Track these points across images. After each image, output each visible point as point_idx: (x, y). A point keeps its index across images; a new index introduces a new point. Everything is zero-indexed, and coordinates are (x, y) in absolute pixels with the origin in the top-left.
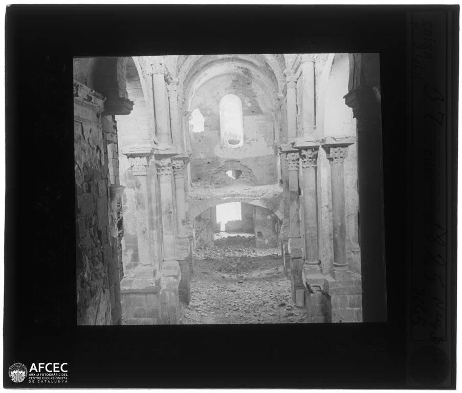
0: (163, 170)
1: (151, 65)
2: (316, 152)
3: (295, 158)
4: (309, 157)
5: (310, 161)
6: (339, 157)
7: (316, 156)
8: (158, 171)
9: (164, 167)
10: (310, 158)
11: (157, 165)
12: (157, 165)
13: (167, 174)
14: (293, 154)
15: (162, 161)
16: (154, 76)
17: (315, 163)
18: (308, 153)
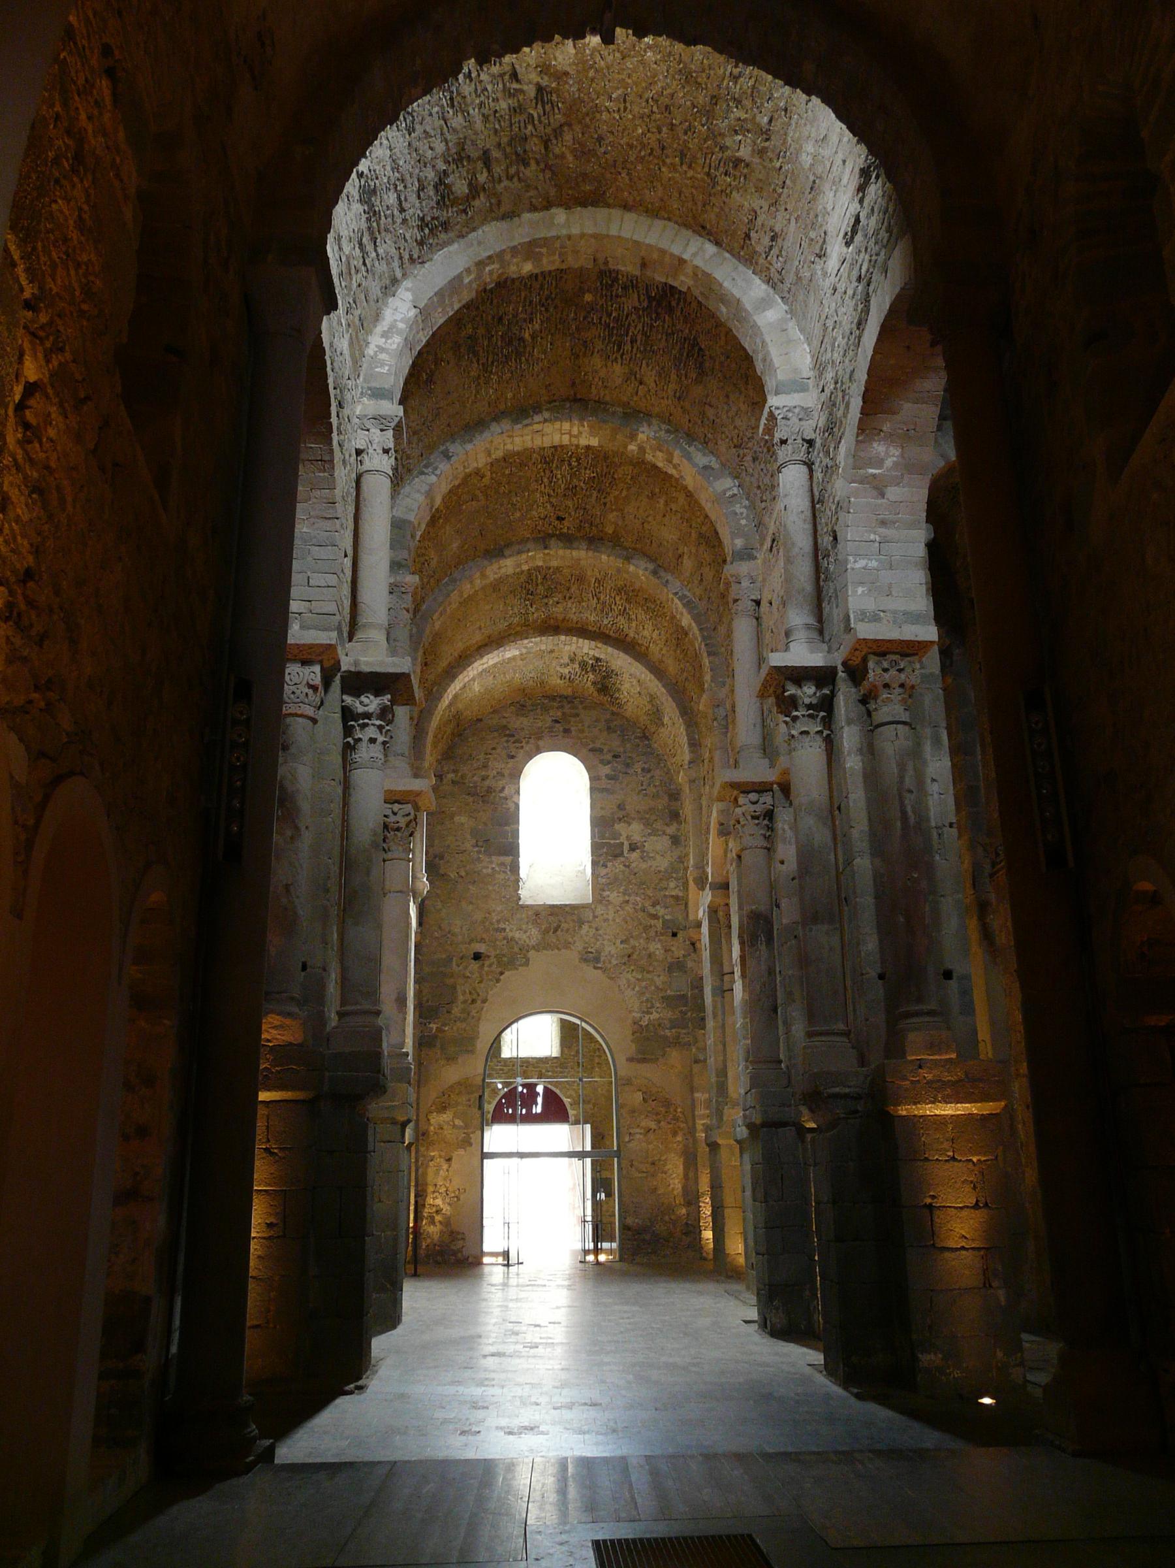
0: (364, 726)
1: (359, 452)
3: (759, 808)
4: (807, 701)
5: (810, 716)
6: (896, 685)
7: (826, 706)
8: (348, 731)
9: (368, 716)
10: (810, 707)
11: (347, 714)
12: (347, 714)
13: (373, 741)
14: (753, 796)
15: (363, 698)
16: (363, 480)
17: (828, 722)
18: (808, 692)
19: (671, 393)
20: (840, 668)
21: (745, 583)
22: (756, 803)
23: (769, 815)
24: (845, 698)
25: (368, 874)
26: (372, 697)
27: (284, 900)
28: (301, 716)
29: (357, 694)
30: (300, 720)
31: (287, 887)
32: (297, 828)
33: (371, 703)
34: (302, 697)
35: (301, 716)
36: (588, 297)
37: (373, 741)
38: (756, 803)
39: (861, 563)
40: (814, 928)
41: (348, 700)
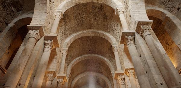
0: (48, 45)
2: (133, 37)
9: (48, 43)
11: (44, 44)
13: (48, 47)
14: (121, 76)
19: (103, 25)
20: (135, 32)
21: (116, 48)
22: (122, 77)
23: (124, 79)
24: (137, 36)
25: (42, 69)
26: (49, 41)
27: (17, 67)
28: (33, 37)
29: (47, 40)
30: (34, 38)
31: (19, 64)
32: (26, 54)
33: (49, 42)
34: (34, 35)
35: (33, 37)
36: (91, 10)
37: (48, 47)
38: (122, 77)
39: (136, 14)
40: (141, 76)
41: (45, 41)
